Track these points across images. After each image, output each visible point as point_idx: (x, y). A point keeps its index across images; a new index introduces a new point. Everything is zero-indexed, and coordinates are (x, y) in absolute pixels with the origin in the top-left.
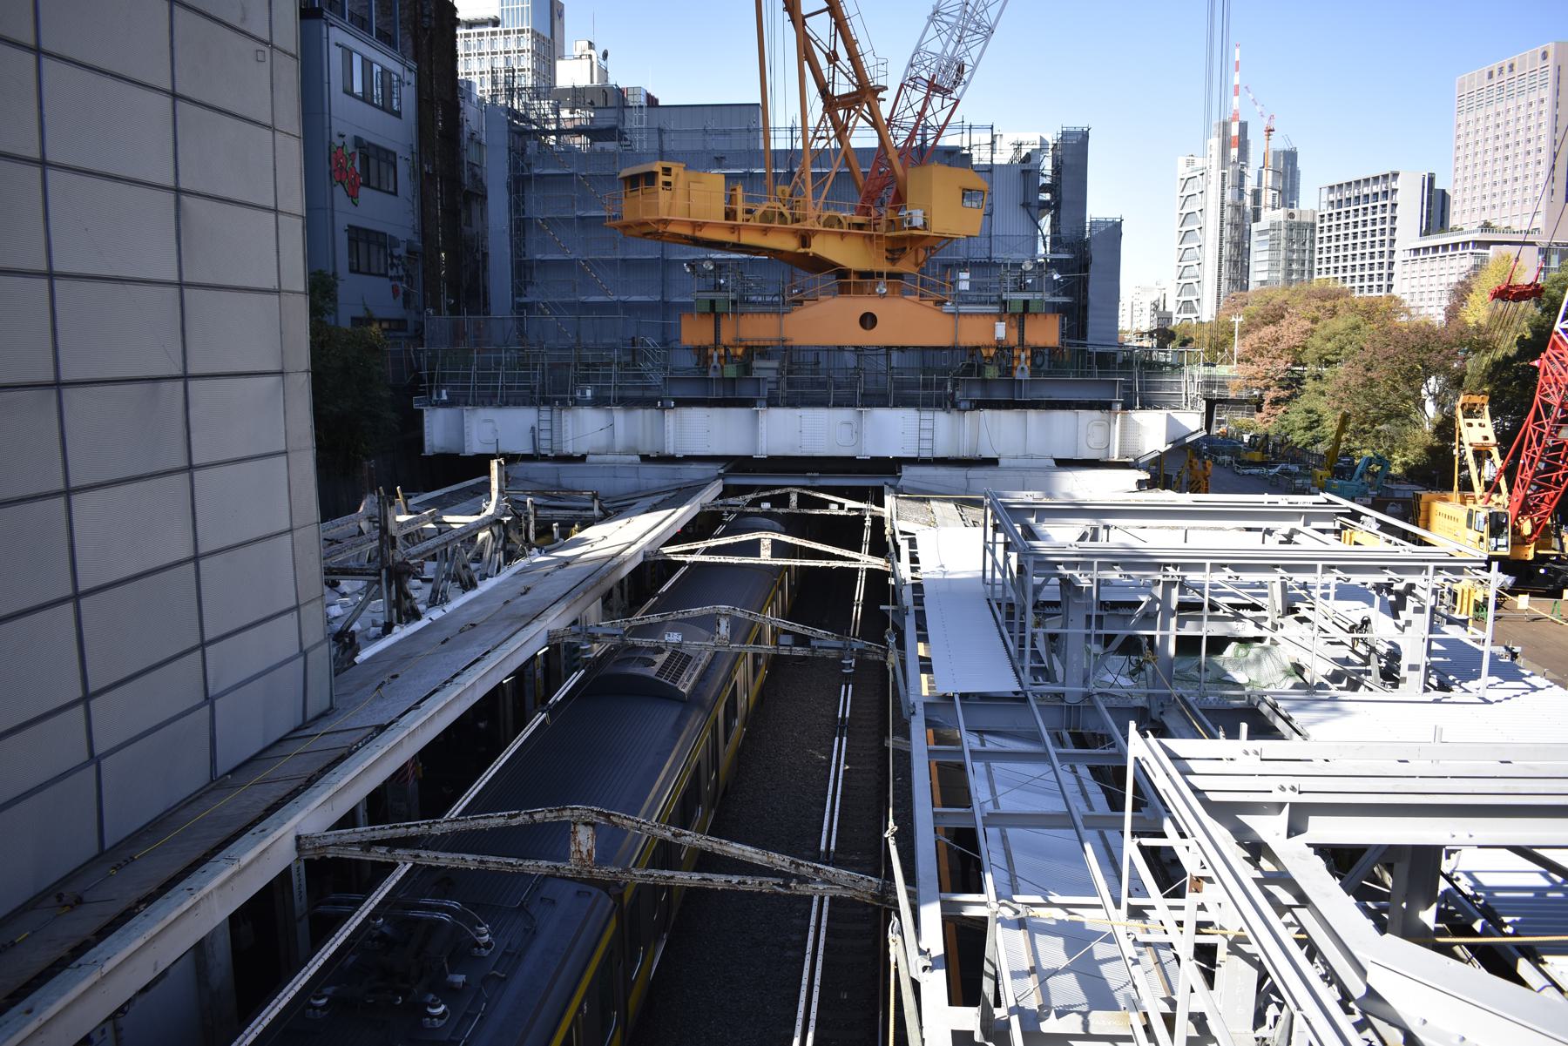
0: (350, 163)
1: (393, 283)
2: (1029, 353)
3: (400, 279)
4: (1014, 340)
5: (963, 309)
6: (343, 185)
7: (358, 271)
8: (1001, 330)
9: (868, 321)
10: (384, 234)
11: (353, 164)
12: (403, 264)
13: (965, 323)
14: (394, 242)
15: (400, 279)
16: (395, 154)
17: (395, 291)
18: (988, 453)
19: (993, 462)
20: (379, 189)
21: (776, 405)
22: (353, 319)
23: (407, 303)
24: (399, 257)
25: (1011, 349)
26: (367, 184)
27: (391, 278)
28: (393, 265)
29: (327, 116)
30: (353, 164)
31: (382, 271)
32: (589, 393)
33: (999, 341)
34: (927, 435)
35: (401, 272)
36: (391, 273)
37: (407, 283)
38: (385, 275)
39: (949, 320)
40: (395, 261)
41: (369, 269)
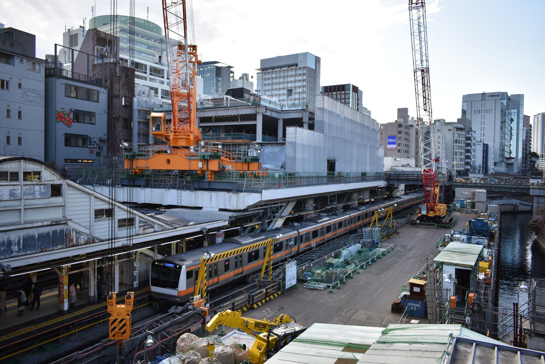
0: (67, 116)
1: (91, 149)
2: (210, 172)
3: (96, 148)
4: (205, 168)
5: (192, 158)
6: (63, 122)
7: (70, 146)
8: (200, 165)
9: (168, 161)
10: (87, 136)
11: (68, 116)
12: (97, 144)
13: (193, 163)
14: (90, 139)
15: (96, 148)
16: (95, 113)
17: (92, 152)
18: (200, 206)
19: (201, 208)
20: (84, 123)
21: (147, 187)
22: (65, 159)
23: (98, 154)
24: (95, 142)
25: (205, 171)
26: (78, 121)
27: (89, 148)
28: (90, 144)
29: (54, 104)
30: (68, 116)
31: (86, 146)
32: (109, 182)
33: (200, 168)
34: (180, 198)
35: (95, 146)
36: (92, 146)
37: (99, 149)
38: (87, 147)
39: (188, 161)
40: (92, 143)
41: (77, 145)
